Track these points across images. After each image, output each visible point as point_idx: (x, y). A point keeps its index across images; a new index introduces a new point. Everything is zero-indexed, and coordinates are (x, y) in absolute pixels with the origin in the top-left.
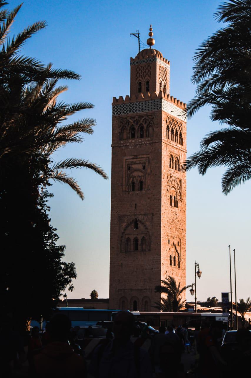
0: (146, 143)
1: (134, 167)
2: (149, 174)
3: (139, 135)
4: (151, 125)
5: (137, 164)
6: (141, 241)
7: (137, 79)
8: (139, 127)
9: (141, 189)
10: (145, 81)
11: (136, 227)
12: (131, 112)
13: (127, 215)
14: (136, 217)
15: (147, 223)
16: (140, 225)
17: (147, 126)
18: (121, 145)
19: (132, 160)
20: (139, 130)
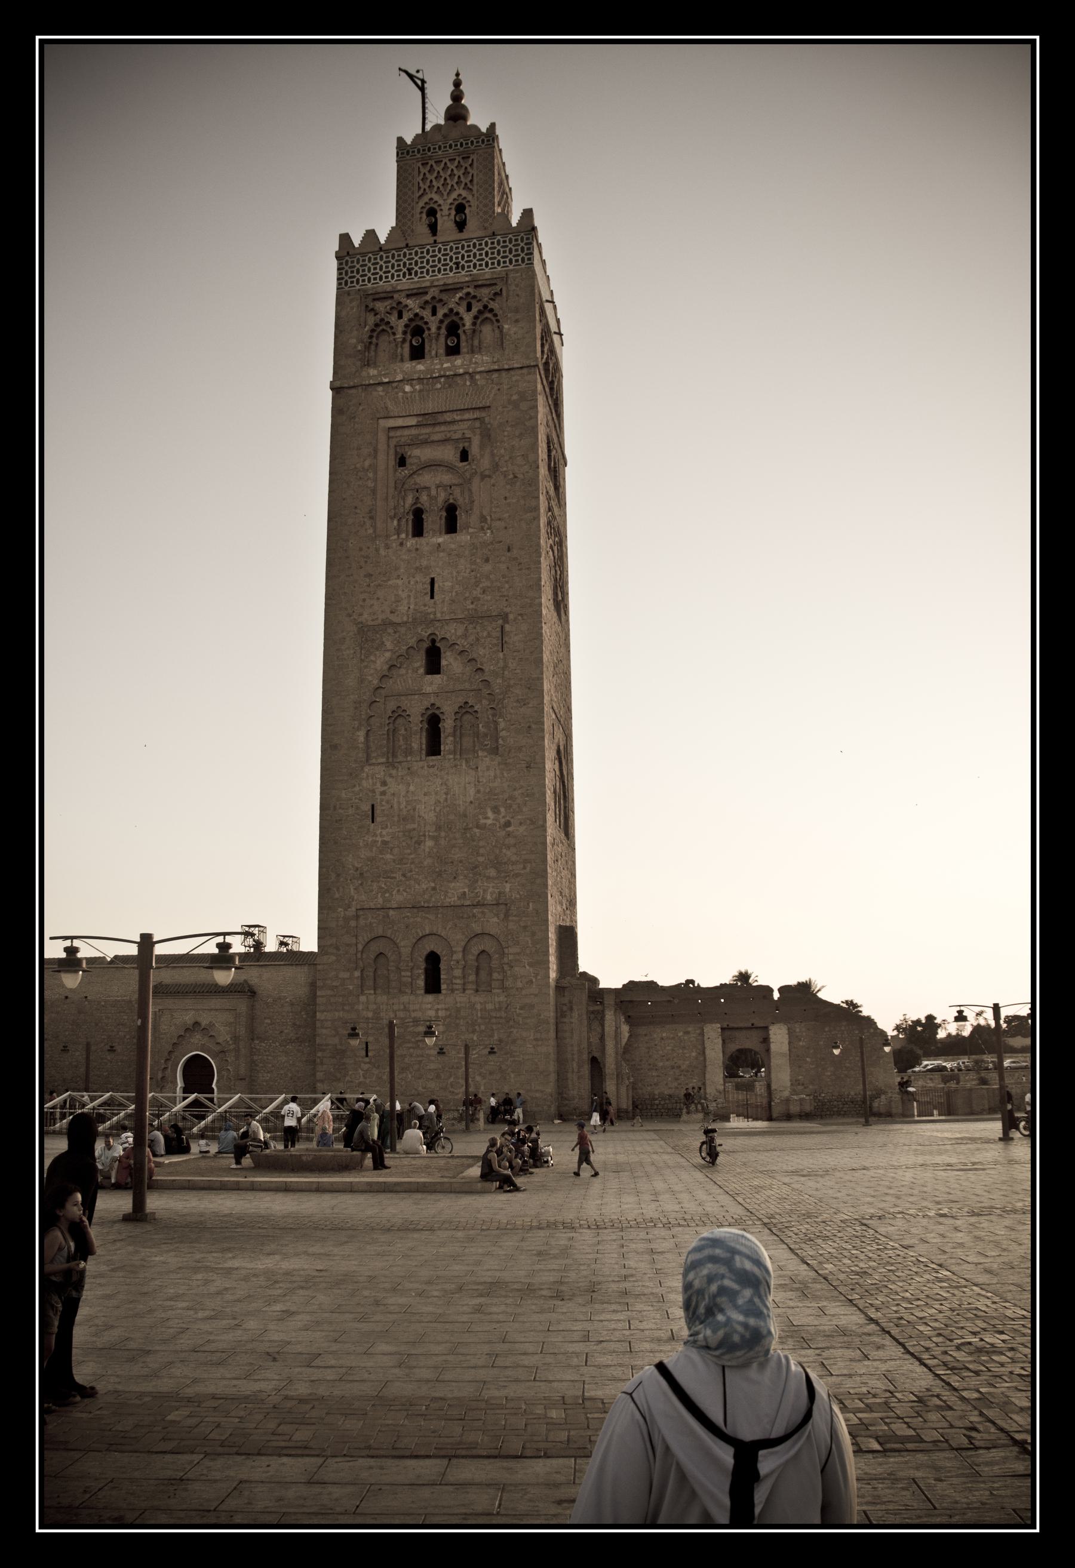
0: (471, 370)
1: (419, 454)
3: (442, 351)
4: (489, 315)
7: (420, 197)
8: (441, 322)
9: (451, 527)
11: (433, 665)
12: (410, 274)
16: (448, 660)
17: (476, 318)
20: (443, 331)
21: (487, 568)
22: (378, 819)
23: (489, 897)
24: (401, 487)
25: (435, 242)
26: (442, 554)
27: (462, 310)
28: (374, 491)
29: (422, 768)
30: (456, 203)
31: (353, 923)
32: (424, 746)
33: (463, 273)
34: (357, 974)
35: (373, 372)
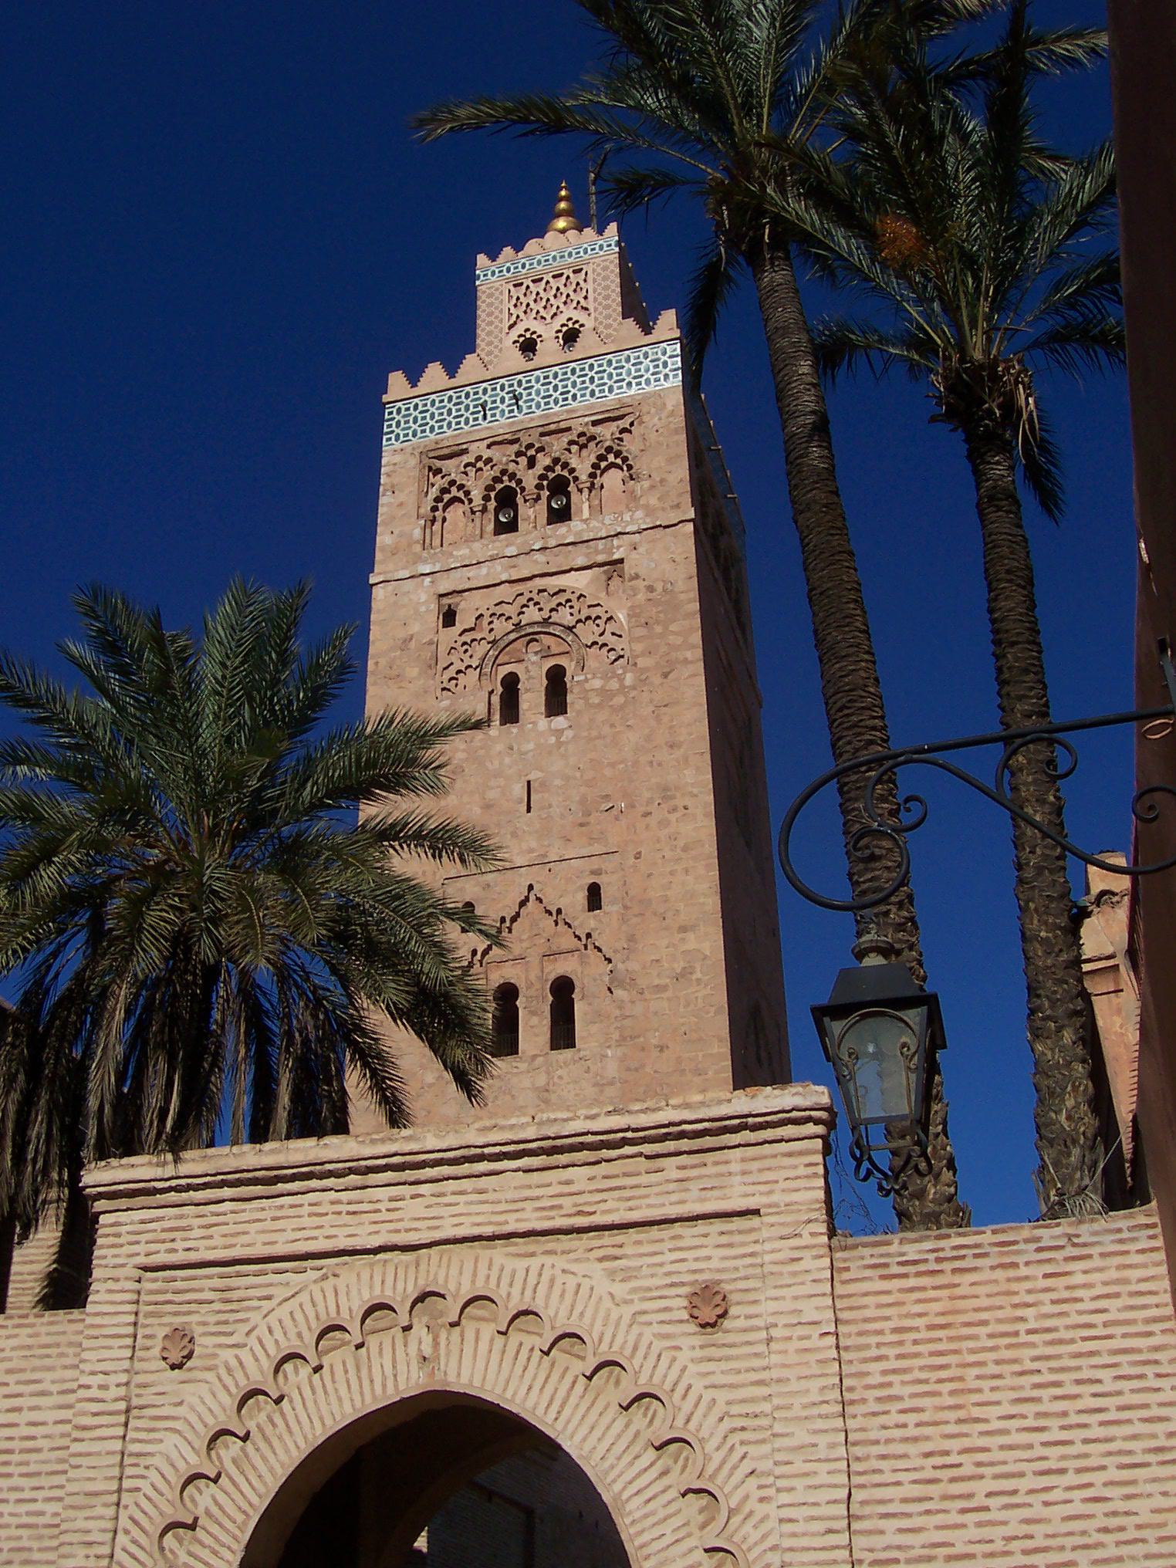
7: (511, 327)
17: (595, 466)
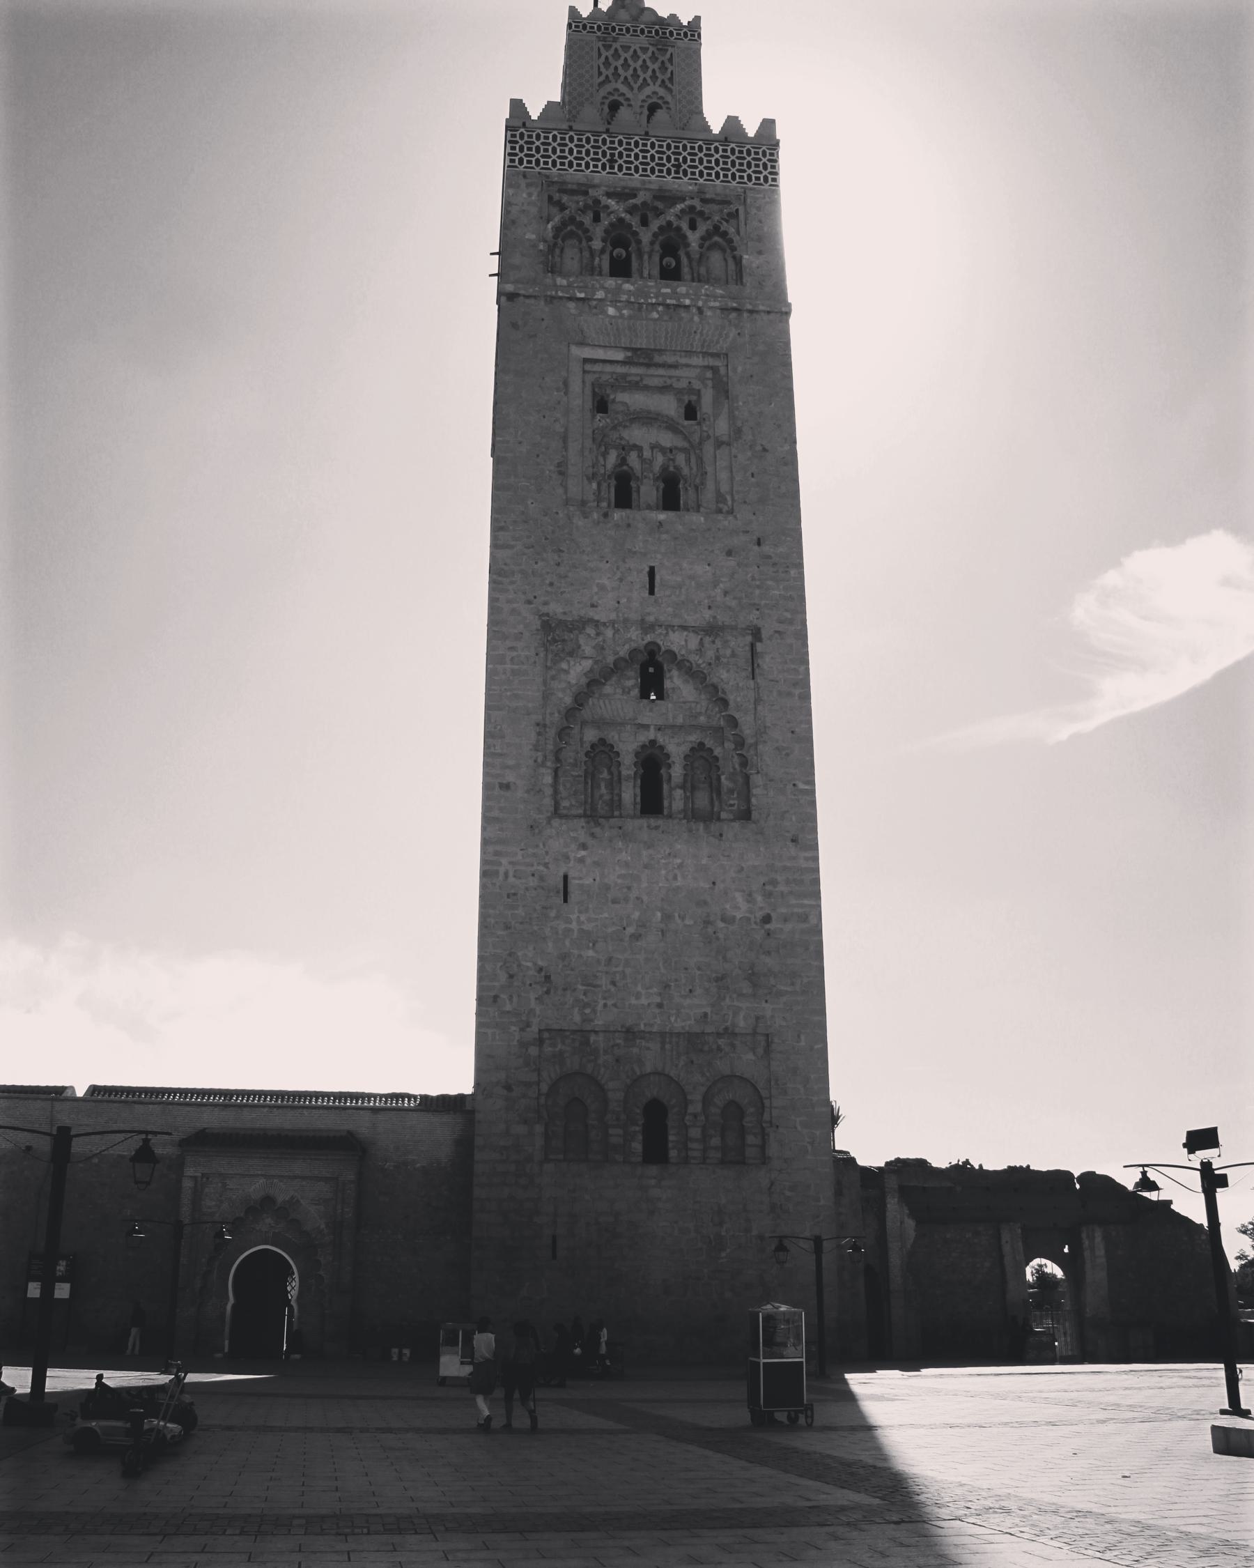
0: (700, 304)
2: (719, 444)
4: (716, 239)
5: (647, 388)
6: (685, 767)
7: (601, 84)
10: (643, 101)
13: (596, 624)
14: (649, 638)
15: (726, 677)
16: (674, 680)
17: (703, 239)
18: (560, 294)
19: (620, 370)
20: (657, 247)
21: (732, 562)
22: (574, 896)
23: (742, 1024)
24: (601, 441)
25: (647, 134)
26: (664, 536)
27: (685, 226)
28: (565, 439)
29: (640, 828)
30: (650, 101)
31: (533, 1051)
32: (638, 799)
33: (686, 179)
34: (539, 1129)
35: (561, 281)
